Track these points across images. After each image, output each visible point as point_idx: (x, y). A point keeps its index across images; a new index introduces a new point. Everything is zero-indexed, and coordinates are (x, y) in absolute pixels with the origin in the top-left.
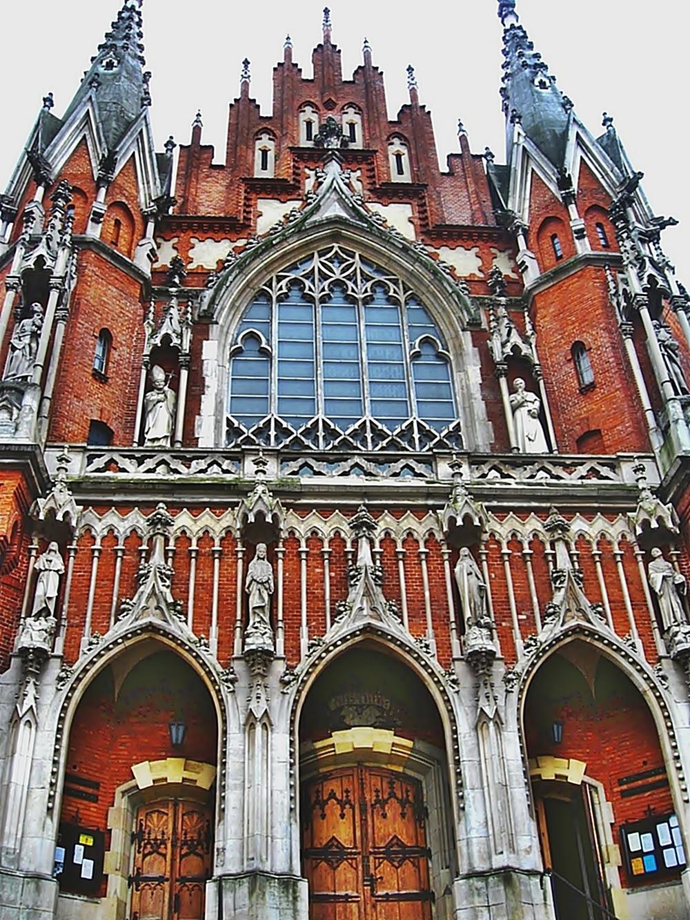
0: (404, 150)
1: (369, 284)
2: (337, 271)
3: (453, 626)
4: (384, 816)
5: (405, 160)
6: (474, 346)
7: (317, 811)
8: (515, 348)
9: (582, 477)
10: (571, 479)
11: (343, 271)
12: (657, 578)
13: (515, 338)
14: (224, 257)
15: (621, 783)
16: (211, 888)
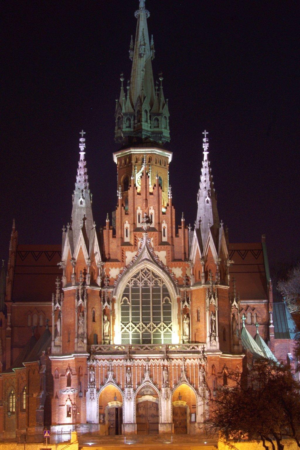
0: (166, 227)
1: (153, 281)
2: (146, 277)
3: (162, 381)
4: (151, 410)
5: (166, 230)
6: (177, 302)
7: (139, 409)
8: (186, 306)
9: (191, 349)
10: (189, 350)
11: (147, 277)
12: (200, 373)
13: (186, 303)
14: (117, 274)
15: (192, 406)
16: (122, 425)
